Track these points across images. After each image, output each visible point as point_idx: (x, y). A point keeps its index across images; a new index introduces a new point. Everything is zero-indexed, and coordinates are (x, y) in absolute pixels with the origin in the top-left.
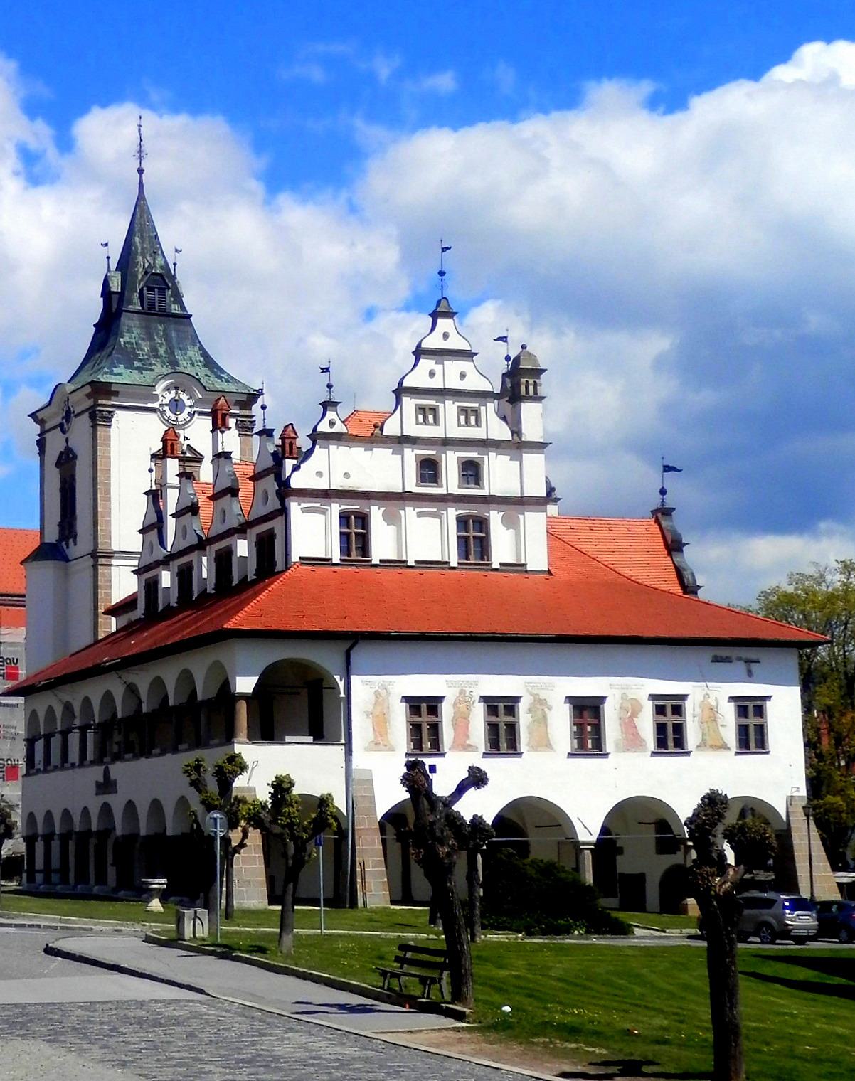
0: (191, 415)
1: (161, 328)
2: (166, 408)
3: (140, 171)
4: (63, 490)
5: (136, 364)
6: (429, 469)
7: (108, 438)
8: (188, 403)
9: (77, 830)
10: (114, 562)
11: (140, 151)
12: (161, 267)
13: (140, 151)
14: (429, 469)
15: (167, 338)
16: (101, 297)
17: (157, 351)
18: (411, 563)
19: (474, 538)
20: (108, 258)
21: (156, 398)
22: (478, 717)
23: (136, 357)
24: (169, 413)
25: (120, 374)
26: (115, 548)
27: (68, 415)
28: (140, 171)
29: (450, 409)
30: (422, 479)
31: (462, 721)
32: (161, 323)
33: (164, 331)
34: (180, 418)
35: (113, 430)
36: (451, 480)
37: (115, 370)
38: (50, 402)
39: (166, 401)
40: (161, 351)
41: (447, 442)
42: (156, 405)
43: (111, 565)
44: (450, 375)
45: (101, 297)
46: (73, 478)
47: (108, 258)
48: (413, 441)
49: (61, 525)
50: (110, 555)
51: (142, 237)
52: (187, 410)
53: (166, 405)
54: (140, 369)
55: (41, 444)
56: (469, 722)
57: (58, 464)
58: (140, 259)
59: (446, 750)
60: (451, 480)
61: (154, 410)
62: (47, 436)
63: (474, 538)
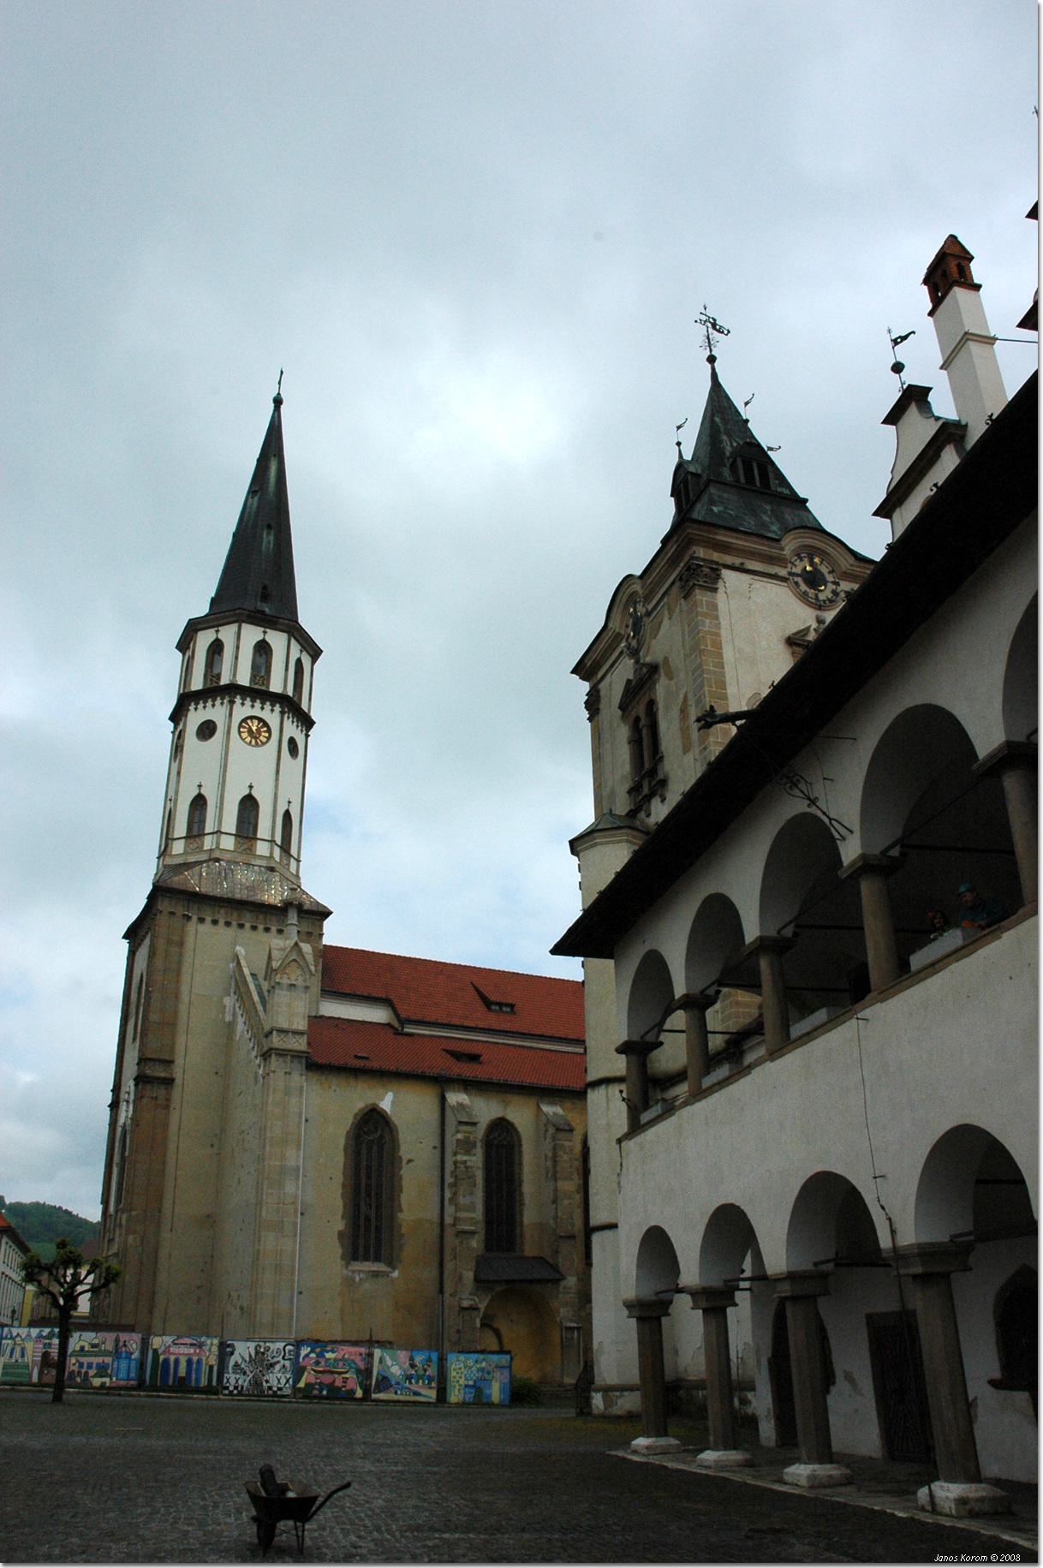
2: (799, 580)
3: (712, 359)
4: (636, 742)
7: (715, 607)
8: (830, 578)
9: (909, 1236)
20: (679, 444)
24: (803, 587)
27: (637, 625)
35: (720, 597)
39: (798, 570)
42: (783, 572)
46: (652, 704)
47: (679, 444)
49: (634, 790)
51: (722, 419)
55: (593, 704)
57: (624, 707)
62: (601, 686)
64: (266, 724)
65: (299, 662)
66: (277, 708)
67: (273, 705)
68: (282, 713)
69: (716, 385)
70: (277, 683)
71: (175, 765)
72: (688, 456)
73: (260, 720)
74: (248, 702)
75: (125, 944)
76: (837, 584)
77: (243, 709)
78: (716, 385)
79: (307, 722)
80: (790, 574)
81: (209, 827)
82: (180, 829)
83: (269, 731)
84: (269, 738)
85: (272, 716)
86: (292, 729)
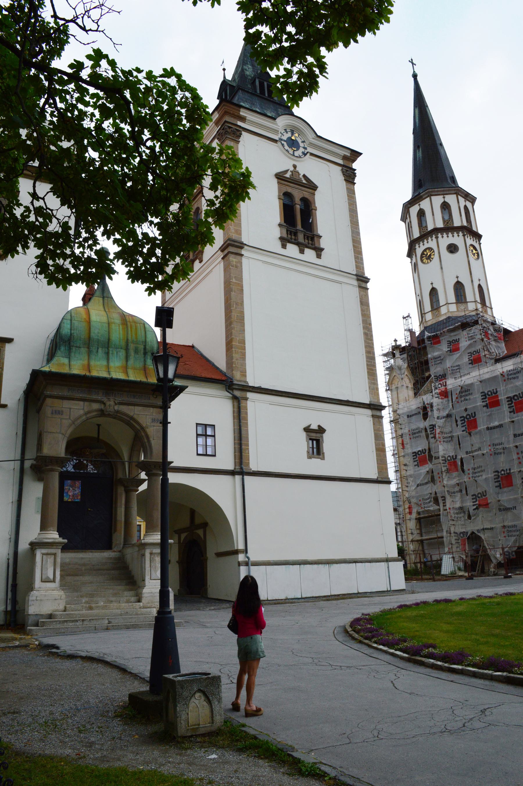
0: (305, 154)
2: (285, 143)
8: (301, 145)
10: (243, 252)
16: (218, 98)
21: (276, 132)
24: (287, 147)
26: (244, 240)
34: (297, 153)
39: (285, 138)
43: (242, 255)
45: (218, 98)
50: (241, 245)
52: (301, 150)
53: (284, 141)
61: (275, 141)
72: (229, 77)
76: (305, 148)
80: (281, 140)
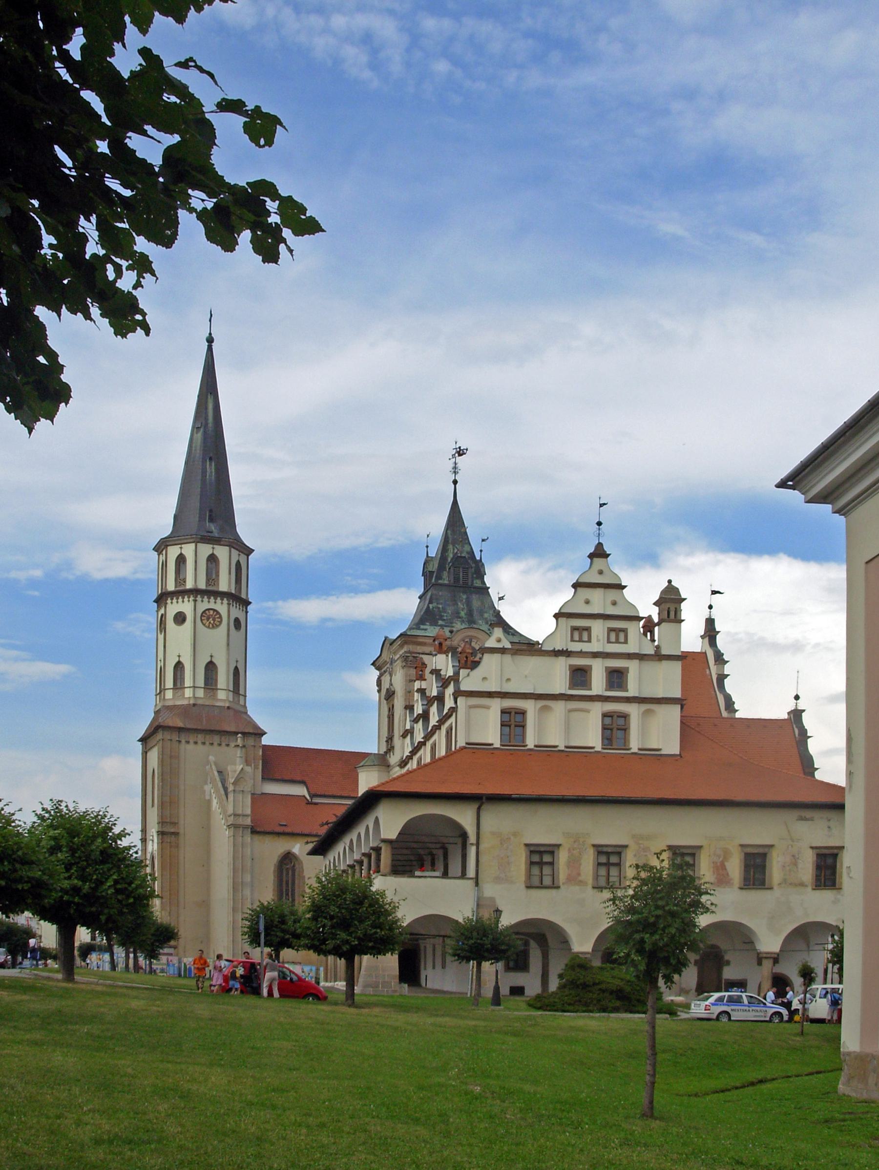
1: (465, 597)
3: (455, 482)
5: (440, 622)
6: (580, 676)
11: (455, 468)
12: (468, 553)
13: (455, 468)
14: (580, 676)
15: (469, 603)
17: (458, 613)
18: (562, 748)
19: (615, 728)
20: (427, 547)
22: (588, 861)
23: (441, 618)
25: (426, 630)
28: (455, 482)
29: (598, 628)
30: (573, 684)
31: (574, 862)
32: (464, 593)
33: (467, 598)
36: (598, 684)
37: (422, 627)
38: (381, 655)
40: (463, 614)
41: (595, 655)
44: (599, 602)
47: (427, 547)
48: (566, 653)
54: (442, 626)
56: (580, 864)
58: (450, 547)
59: (561, 884)
60: (598, 684)
63: (615, 728)
64: (218, 613)
65: (238, 565)
66: (225, 601)
67: (222, 600)
68: (229, 604)
69: (455, 503)
70: (224, 584)
71: (161, 637)
73: (214, 610)
74: (206, 599)
75: (139, 746)
77: (205, 604)
78: (455, 503)
79: (247, 603)
81: (188, 682)
82: (169, 683)
83: (221, 617)
84: (221, 622)
85: (222, 607)
86: (236, 612)
